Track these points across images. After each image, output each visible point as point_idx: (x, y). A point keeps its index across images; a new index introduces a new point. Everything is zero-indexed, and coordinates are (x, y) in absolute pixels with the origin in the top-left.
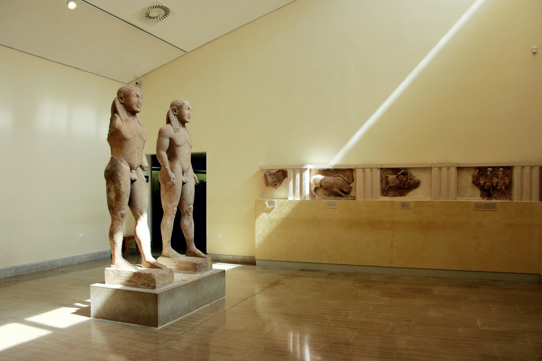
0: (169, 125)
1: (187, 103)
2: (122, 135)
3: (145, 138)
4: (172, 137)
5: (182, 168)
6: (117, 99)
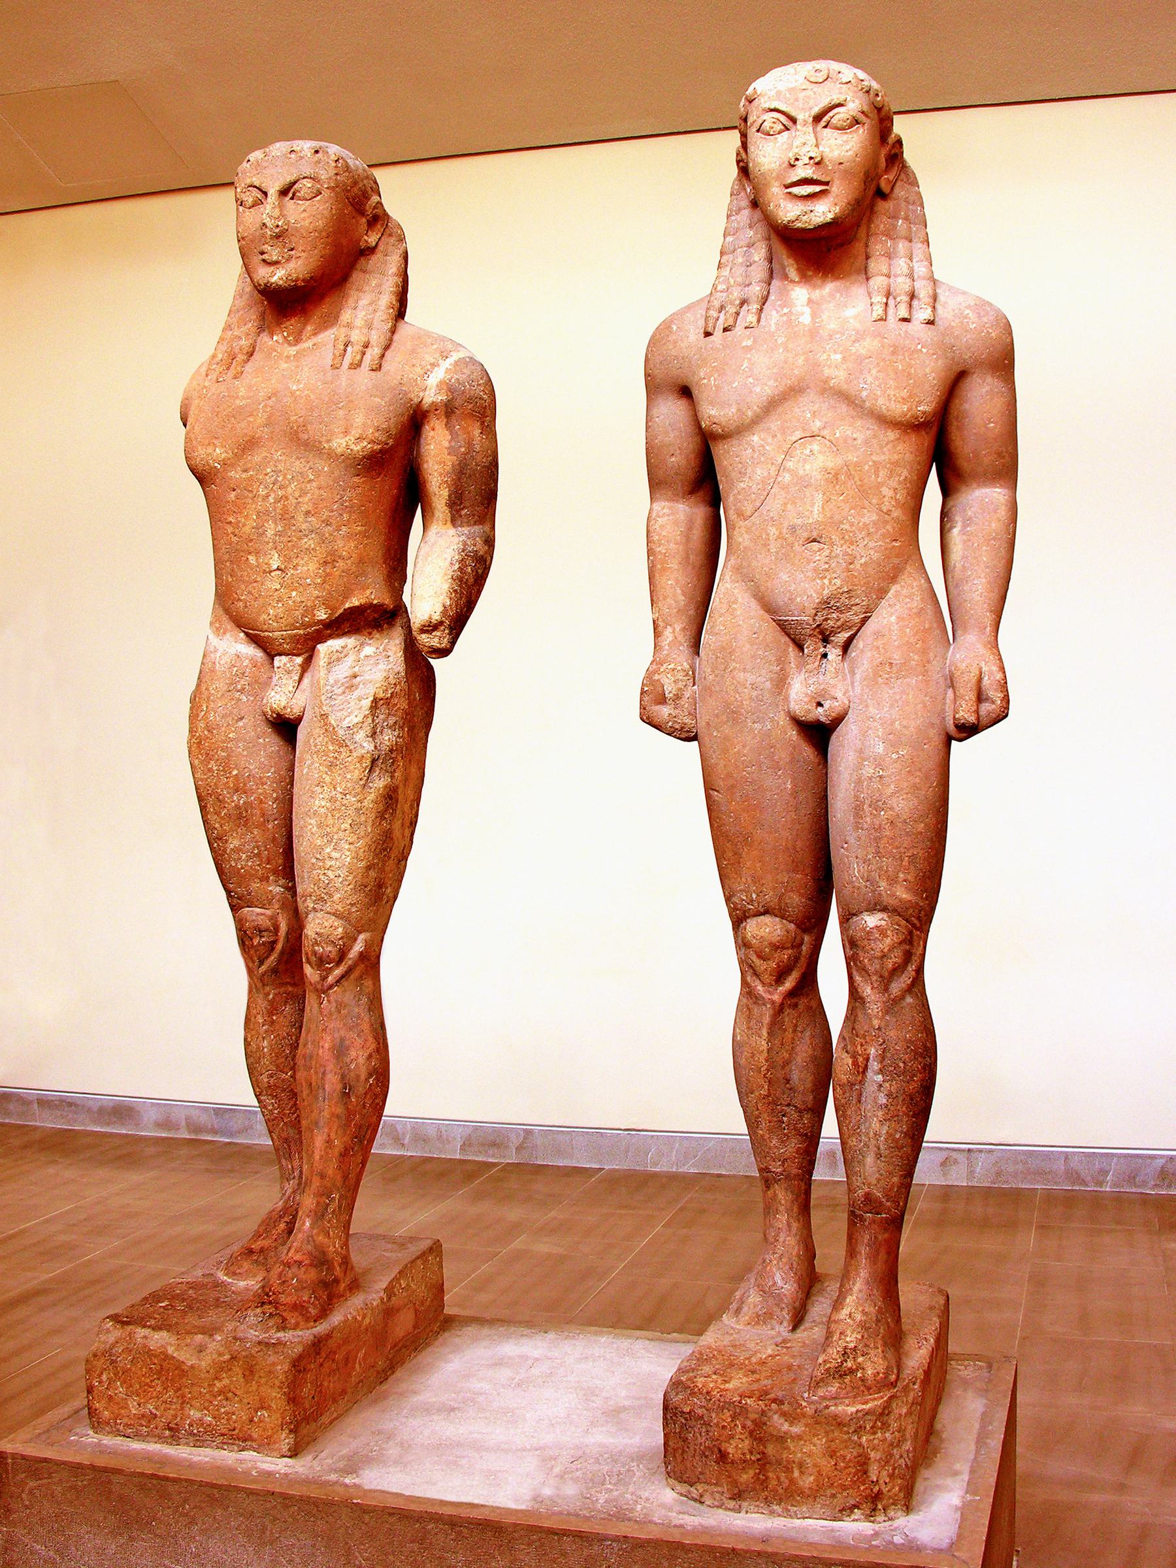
5: (769, 608)
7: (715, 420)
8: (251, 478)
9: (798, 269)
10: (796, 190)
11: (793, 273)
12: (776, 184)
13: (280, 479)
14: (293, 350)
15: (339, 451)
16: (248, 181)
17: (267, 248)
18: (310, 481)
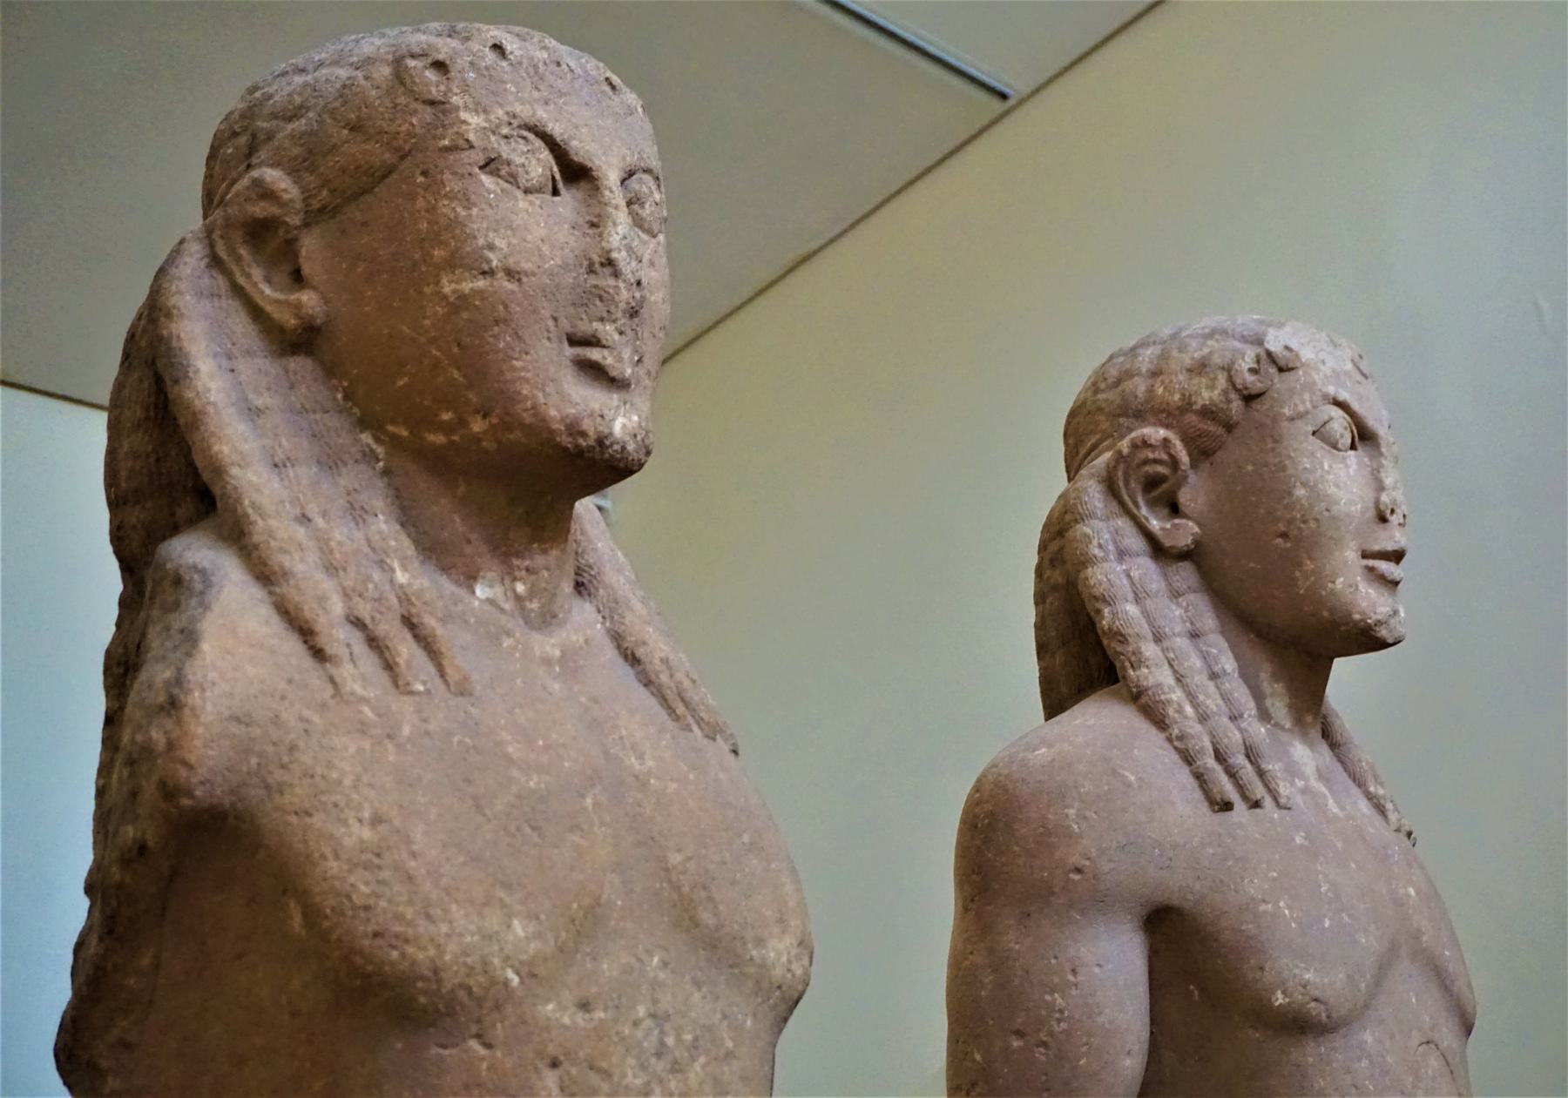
0: (1098, 719)
1: (1324, 359)
2: (311, 914)
3: (778, 952)
4: (1177, 884)
6: (193, 261)
7: (1317, 993)
8: (600, 1032)
9: (1290, 707)
10: (1384, 566)
11: (1279, 707)
12: (1353, 544)
13: (670, 1041)
14: (548, 645)
15: (778, 972)
16: (524, 111)
17: (608, 331)
18: (729, 1055)
